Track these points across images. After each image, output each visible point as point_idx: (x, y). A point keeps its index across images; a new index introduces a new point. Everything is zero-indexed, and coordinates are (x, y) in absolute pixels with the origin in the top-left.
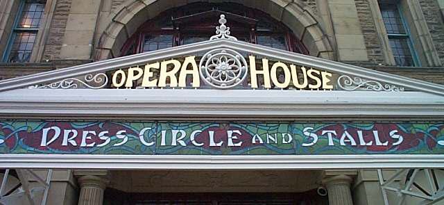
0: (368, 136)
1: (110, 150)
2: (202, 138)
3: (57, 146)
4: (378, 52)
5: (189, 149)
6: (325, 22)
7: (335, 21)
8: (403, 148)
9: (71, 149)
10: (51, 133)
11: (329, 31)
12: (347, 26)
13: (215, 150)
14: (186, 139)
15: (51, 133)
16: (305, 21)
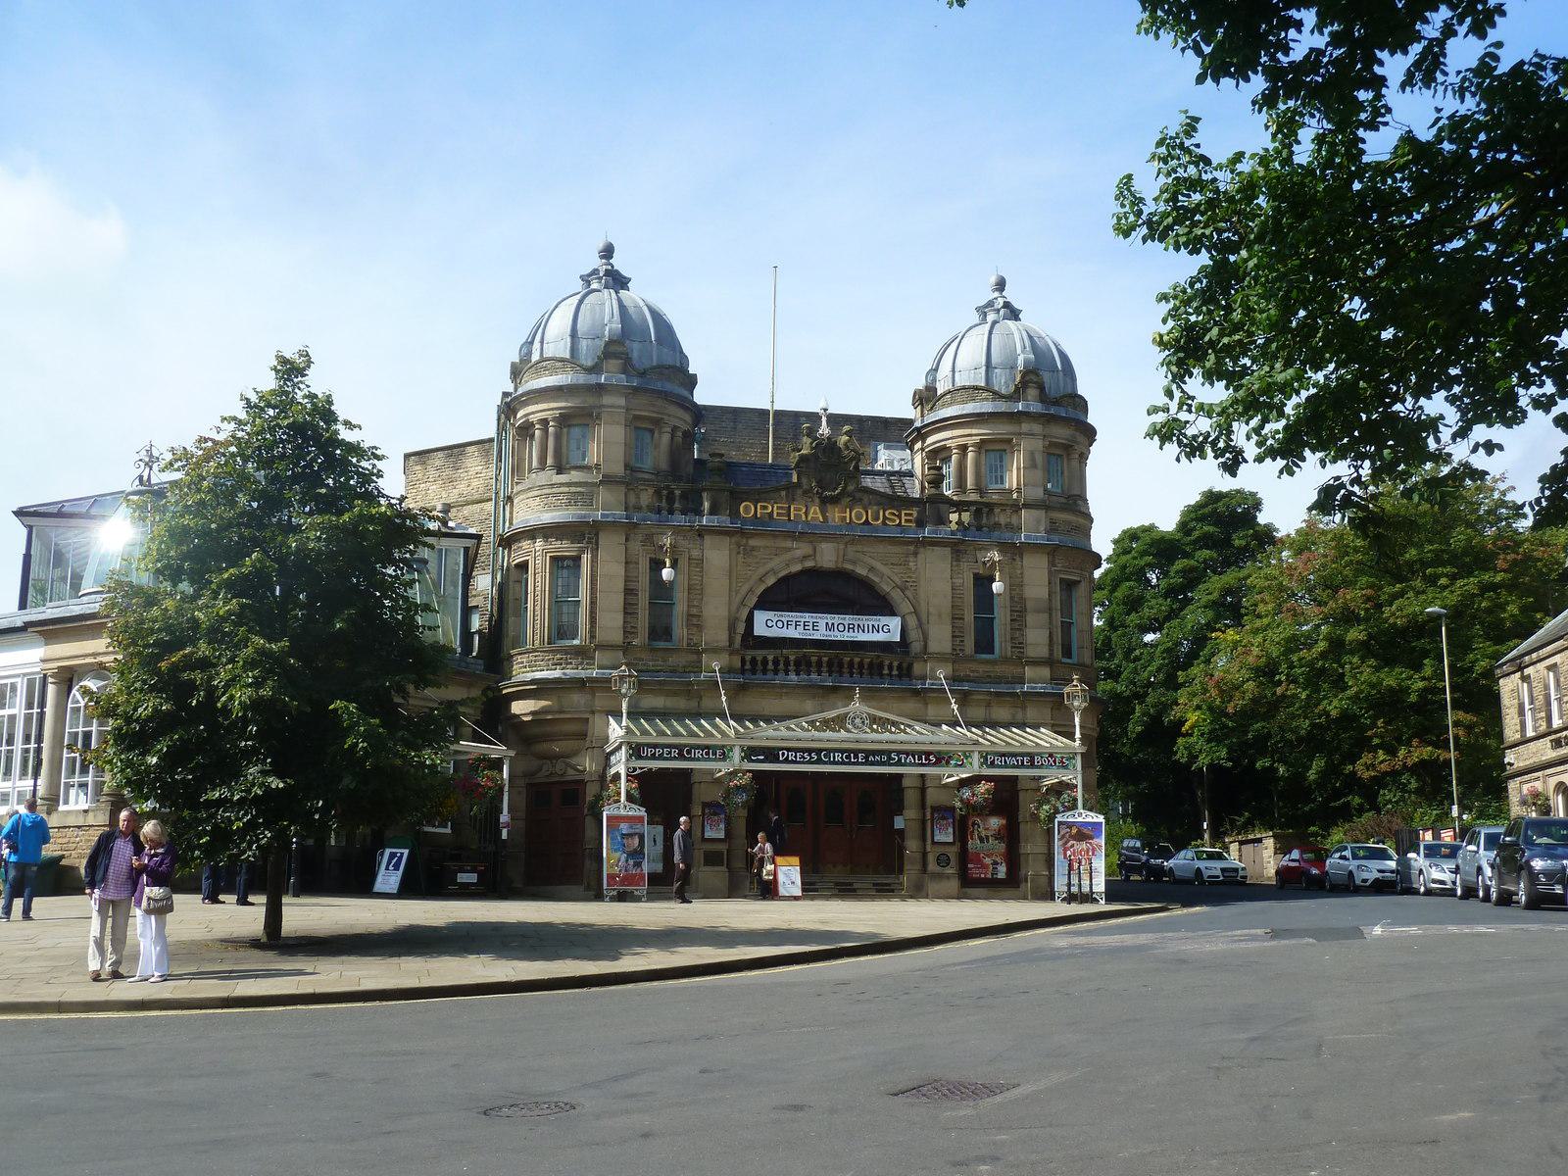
0: (920, 758)
1: (810, 762)
2: (848, 757)
3: (786, 761)
4: (962, 641)
5: (843, 763)
6: (923, 608)
7: (931, 610)
8: (935, 764)
9: (795, 762)
10: (783, 754)
11: (924, 618)
12: (940, 616)
13: (854, 764)
14: (842, 758)
15: (783, 754)
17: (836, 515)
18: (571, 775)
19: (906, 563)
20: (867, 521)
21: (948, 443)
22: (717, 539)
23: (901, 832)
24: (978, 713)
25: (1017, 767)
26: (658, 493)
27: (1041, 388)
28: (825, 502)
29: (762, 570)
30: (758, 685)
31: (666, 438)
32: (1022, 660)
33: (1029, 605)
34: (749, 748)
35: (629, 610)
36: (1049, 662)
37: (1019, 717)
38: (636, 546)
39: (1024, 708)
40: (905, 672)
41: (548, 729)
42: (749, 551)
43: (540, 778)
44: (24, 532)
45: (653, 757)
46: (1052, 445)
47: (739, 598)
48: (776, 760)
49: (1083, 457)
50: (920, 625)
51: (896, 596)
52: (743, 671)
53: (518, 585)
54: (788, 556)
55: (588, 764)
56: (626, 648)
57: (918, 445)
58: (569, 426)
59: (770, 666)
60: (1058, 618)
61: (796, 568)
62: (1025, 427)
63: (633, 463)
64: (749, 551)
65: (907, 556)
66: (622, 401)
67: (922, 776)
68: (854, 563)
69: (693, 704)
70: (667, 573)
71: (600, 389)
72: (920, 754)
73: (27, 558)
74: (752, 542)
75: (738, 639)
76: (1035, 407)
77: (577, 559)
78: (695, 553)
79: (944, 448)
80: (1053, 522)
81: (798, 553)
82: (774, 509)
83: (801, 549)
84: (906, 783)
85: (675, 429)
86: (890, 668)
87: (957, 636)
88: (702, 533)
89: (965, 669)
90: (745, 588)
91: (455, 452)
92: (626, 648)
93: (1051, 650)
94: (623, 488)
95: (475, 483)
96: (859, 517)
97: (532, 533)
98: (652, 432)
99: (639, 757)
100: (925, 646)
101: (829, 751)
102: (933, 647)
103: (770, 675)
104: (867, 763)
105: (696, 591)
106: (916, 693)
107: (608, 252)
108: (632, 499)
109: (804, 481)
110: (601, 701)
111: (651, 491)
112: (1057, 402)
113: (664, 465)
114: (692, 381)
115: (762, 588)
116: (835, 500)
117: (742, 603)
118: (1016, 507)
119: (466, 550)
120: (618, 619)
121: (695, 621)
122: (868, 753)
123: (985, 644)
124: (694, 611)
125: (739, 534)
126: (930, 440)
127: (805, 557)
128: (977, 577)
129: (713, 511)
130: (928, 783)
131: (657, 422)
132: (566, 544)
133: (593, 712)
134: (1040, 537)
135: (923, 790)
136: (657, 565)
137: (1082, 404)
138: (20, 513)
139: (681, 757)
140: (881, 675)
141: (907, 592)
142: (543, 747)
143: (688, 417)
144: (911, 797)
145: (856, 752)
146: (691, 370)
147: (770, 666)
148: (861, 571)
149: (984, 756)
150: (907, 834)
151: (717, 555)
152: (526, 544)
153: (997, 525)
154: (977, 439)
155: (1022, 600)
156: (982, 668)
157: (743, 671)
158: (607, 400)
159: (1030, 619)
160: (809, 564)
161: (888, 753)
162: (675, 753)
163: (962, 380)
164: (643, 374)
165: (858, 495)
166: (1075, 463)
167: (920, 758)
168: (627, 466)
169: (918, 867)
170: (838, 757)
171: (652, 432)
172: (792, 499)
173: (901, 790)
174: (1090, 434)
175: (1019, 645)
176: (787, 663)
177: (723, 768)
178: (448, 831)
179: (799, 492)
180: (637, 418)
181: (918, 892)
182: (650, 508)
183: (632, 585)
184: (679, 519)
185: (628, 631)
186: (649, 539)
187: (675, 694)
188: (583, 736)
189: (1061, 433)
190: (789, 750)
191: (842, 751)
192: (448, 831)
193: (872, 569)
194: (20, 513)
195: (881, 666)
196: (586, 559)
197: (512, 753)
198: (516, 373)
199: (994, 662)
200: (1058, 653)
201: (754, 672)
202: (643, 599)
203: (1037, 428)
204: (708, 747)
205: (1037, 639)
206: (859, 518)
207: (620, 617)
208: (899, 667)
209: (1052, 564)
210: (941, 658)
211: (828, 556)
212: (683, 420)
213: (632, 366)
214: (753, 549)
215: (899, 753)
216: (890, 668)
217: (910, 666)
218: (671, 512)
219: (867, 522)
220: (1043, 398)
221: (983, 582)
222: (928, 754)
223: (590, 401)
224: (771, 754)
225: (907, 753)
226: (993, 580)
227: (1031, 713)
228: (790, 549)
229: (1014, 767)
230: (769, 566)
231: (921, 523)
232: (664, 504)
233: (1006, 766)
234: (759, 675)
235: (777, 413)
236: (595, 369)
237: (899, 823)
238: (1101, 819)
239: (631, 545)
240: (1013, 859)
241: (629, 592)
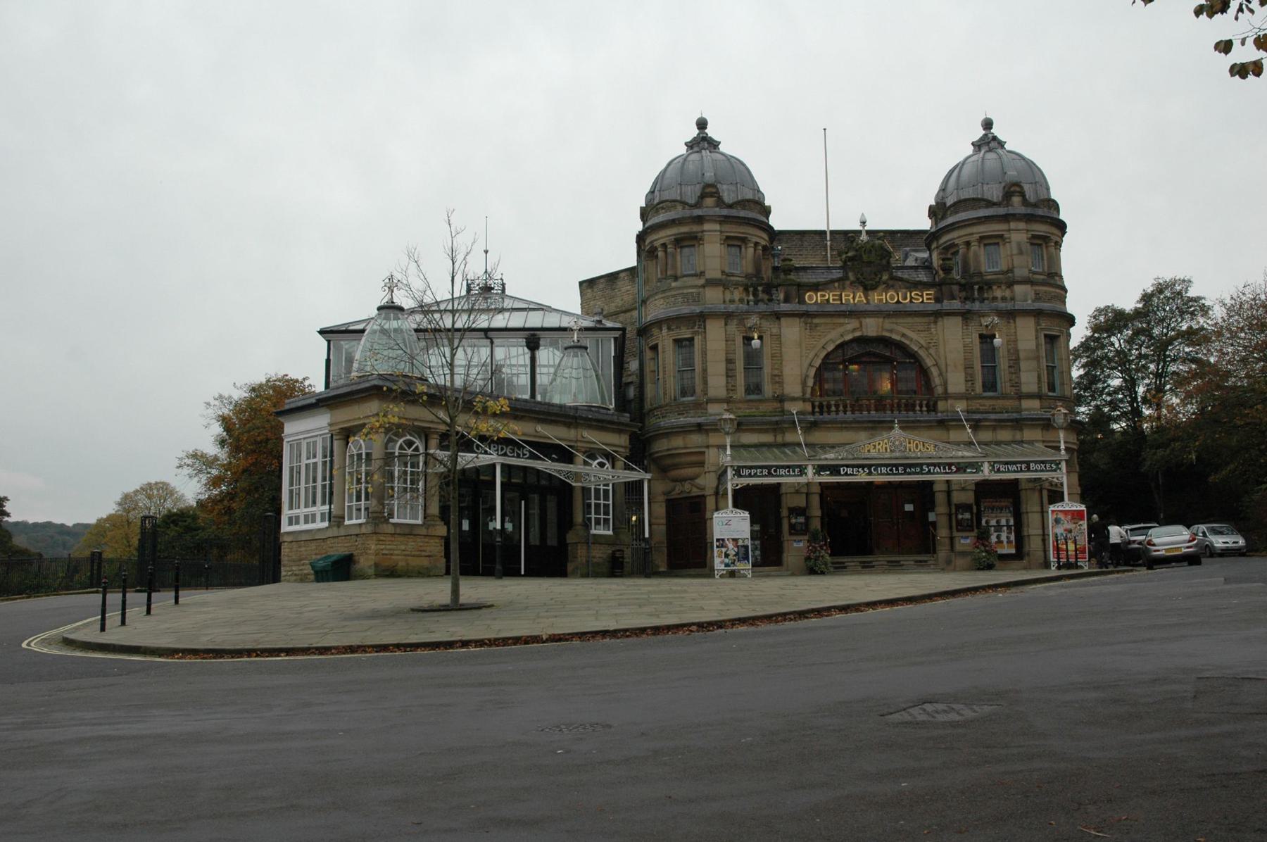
3: (846, 474)
11: (943, 367)
16: (929, 362)
17: (876, 297)
18: (695, 492)
19: (929, 329)
20: (898, 302)
21: (956, 242)
22: (790, 320)
23: (934, 524)
24: (986, 435)
26: (746, 290)
27: (1022, 194)
28: (867, 289)
29: (823, 341)
30: (826, 423)
31: (751, 250)
32: (1021, 396)
33: (1022, 355)
35: (730, 374)
36: (1039, 396)
37: (1018, 437)
38: (733, 327)
39: (1021, 430)
40: (932, 408)
41: (677, 460)
42: (813, 328)
43: (674, 495)
44: (326, 343)
45: (750, 475)
46: (1034, 237)
47: (808, 361)
49: (1058, 245)
50: (941, 374)
51: (922, 353)
52: (813, 413)
53: (652, 363)
54: (841, 330)
55: (708, 482)
56: (728, 401)
57: (934, 246)
58: (682, 247)
59: (833, 408)
60: (1044, 363)
61: (849, 337)
62: (1013, 225)
63: (727, 270)
64: (813, 328)
65: (929, 323)
66: (717, 227)
67: (948, 481)
68: (891, 331)
69: (779, 439)
70: (756, 343)
71: (700, 220)
72: (945, 465)
73: (328, 361)
74: (816, 321)
75: (809, 390)
76: (1022, 210)
77: (691, 340)
78: (775, 331)
79: (953, 245)
80: (1037, 294)
81: (849, 327)
82: (830, 296)
83: (852, 324)
84: (936, 488)
86: (921, 406)
87: (970, 379)
88: (778, 316)
89: (975, 405)
90: (811, 355)
91: (612, 277)
92: (728, 401)
93: (1040, 388)
94: (721, 289)
95: (626, 298)
96: (892, 298)
97: (658, 323)
98: (740, 247)
99: (740, 476)
100: (946, 389)
101: (878, 466)
102: (951, 389)
103: (833, 415)
104: (905, 473)
105: (778, 357)
106: (942, 424)
107: (702, 124)
108: (728, 296)
109: (851, 276)
110: (714, 439)
111: (741, 289)
112: (1035, 205)
113: (750, 270)
114: (767, 211)
115: (824, 353)
116: (874, 288)
117: (810, 365)
118: (1010, 285)
119: (616, 339)
120: (722, 381)
121: (778, 379)
122: (906, 466)
123: (990, 385)
124: (776, 372)
125: (805, 315)
126: (941, 241)
127: (854, 330)
128: (981, 336)
129: (787, 300)
130: (954, 487)
131: (744, 240)
132: (684, 330)
133: (708, 447)
134: (1030, 304)
135: (949, 493)
136: (748, 339)
137: (1054, 206)
138: (322, 332)
139: (770, 474)
140: (914, 410)
141: (932, 351)
142: (675, 473)
143: (765, 236)
144: (940, 498)
145: (897, 466)
146: (767, 203)
147: (833, 408)
148: (896, 337)
149: (992, 465)
150: (938, 525)
151: (791, 331)
152: (655, 331)
153: (995, 299)
154: (977, 236)
155: (1017, 351)
156: (988, 403)
157: (813, 413)
158: (707, 227)
159: (1023, 365)
160: (858, 334)
161: (921, 465)
162: (765, 472)
163: (965, 194)
164: (730, 206)
165: (891, 282)
166: (1052, 250)
168: (723, 272)
169: (948, 547)
170: (884, 470)
171: (740, 247)
172: (844, 289)
173: (932, 494)
174: (1062, 227)
175: (1017, 385)
176: (845, 407)
177: (803, 480)
178: (611, 533)
179: (848, 283)
180: (728, 238)
181: (948, 566)
182: (741, 301)
183: (731, 356)
184: (762, 307)
185: (731, 388)
186: (741, 322)
187: (766, 431)
188: (702, 464)
189: (1041, 229)
190: (848, 466)
191: (886, 466)
192: (611, 533)
193: (903, 335)
194: (322, 332)
195: (914, 406)
196: (697, 340)
197: (648, 476)
198: (644, 214)
199: (997, 398)
200: (1045, 389)
201: (821, 413)
202: (740, 365)
203: (1022, 225)
204: (788, 467)
205: (1029, 382)
206: (892, 298)
207: (724, 379)
208: (927, 405)
209: (1038, 324)
210: (959, 397)
211: (871, 327)
212: (763, 239)
213: (723, 202)
214: (816, 325)
215: (928, 465)
216: (921, 406)
217: (935, 404)
218: (756, 302)
219: (898, 302)
220: (1025, 202)
221: (986, 338)
222: (950, 465)
223: (695, 228)
224: (835, 470)
225: (935, 465)
226: (994, 336)
227: (1028, 434)
230: (829, 337)
232: (751, 297)
233: (1009, 471)
234: (826, 417)
235: (832, 232)
237: (932, 517)
238: (1083, 507)
239: (729, 327)
240: (1020, 542)
241: (729, 361)
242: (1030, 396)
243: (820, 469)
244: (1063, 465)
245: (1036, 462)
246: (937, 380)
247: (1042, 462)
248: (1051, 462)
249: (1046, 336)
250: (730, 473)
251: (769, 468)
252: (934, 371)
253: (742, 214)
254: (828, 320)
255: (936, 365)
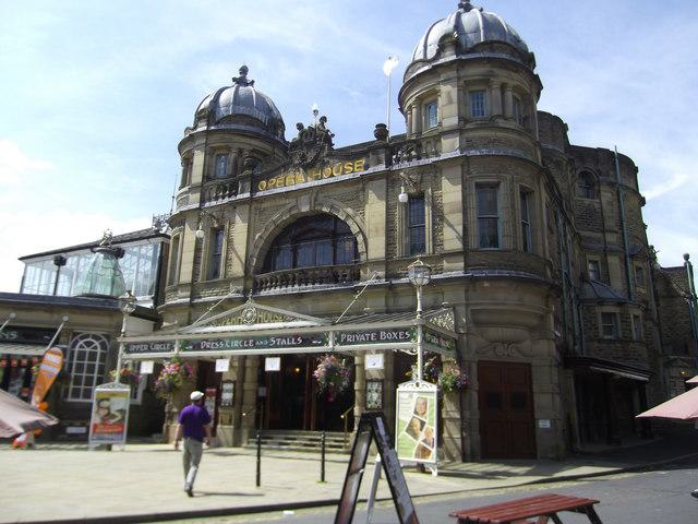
0: (291, 340)
2: (243, 343)
3: (205, 349)
9: (209, 349)
13: (246, 348)
25: (365, 342)
34: (185, 340)
42: (261, 212)
48: (199, 349)
73: (23, 278)
74: (264, 205)
85: (241, 151)
104: (255, 347)
122: (255, 339)
161: (268, 338)
167: (291, 340)
175: (437, 242)
190: (207, 340)
194: (20, 259)
203: (452, 74)
215: (276, 337)
222: (296, 336)
228: (284, 205)
229: (363, 342)
231: (366, 167)
233: (356, 342)
236: (195, 128)
242: (452, 255)
243: (185, 345)
244: (419, 330)
245: (387, 330)
246: (361, 248)
247: (395, 330)
248: (405, 330)
249: (477, 185)
250: (121, 349)
251: (147, 343)
252: (360, 239)
253: (234, 126)
254: (273, 203)
255: (361, 231)
